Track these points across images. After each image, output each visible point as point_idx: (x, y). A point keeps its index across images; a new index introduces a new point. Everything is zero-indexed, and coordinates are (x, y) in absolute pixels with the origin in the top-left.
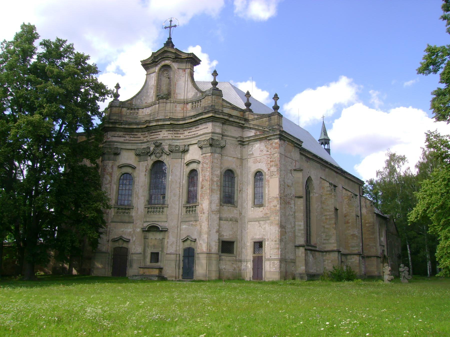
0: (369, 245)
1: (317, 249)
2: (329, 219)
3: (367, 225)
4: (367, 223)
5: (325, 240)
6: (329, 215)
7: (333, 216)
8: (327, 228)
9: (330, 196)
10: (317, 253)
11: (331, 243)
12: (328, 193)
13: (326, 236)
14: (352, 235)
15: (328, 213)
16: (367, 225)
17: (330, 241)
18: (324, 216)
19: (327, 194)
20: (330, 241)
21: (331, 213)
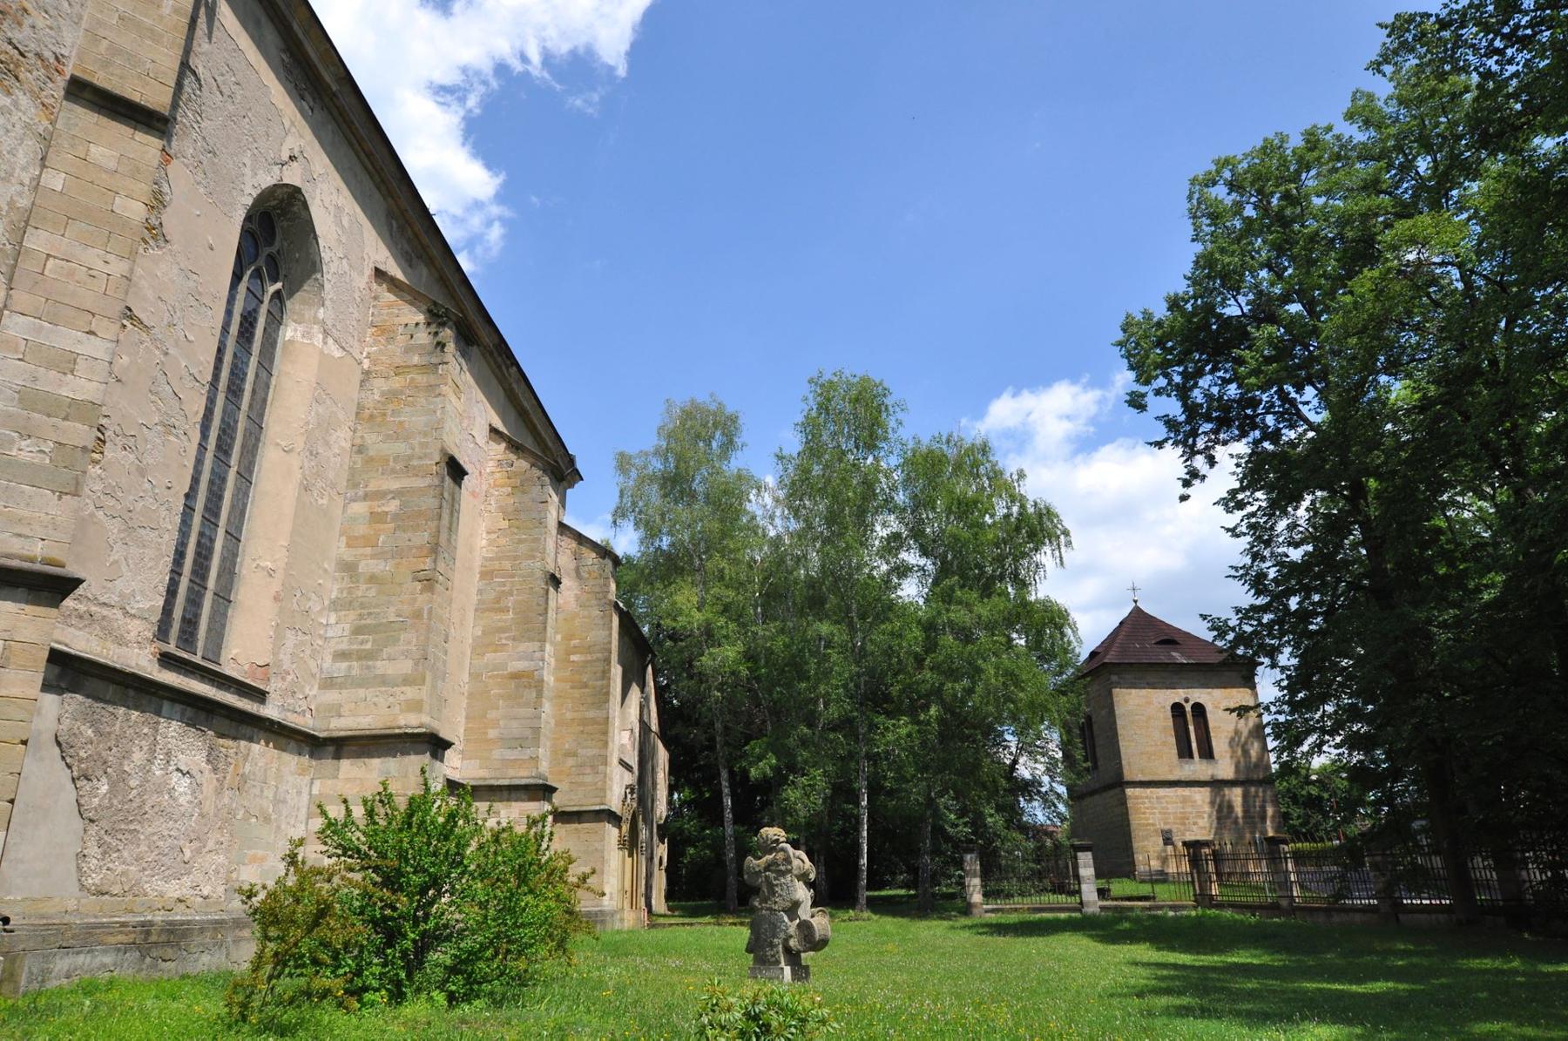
0: (575, 755)
1: (270, 711)
2: (396, 517)
3: (573, 658)
4: (575, 650)
5: (342, 656)
6: (398, 494)
7: (430, 502)
8: (372, 579)
9: (422, 379)
10: (259, 753)
11: (384, 681)
12: (416, 359)
13: (357, 631)
14: (515, 676)
15: (395, 485)
16: (573, 658)
17: (382, 667)
18: (366, 497)
19: (399, 370)
20: (382, 667)
21: (420, 483)
